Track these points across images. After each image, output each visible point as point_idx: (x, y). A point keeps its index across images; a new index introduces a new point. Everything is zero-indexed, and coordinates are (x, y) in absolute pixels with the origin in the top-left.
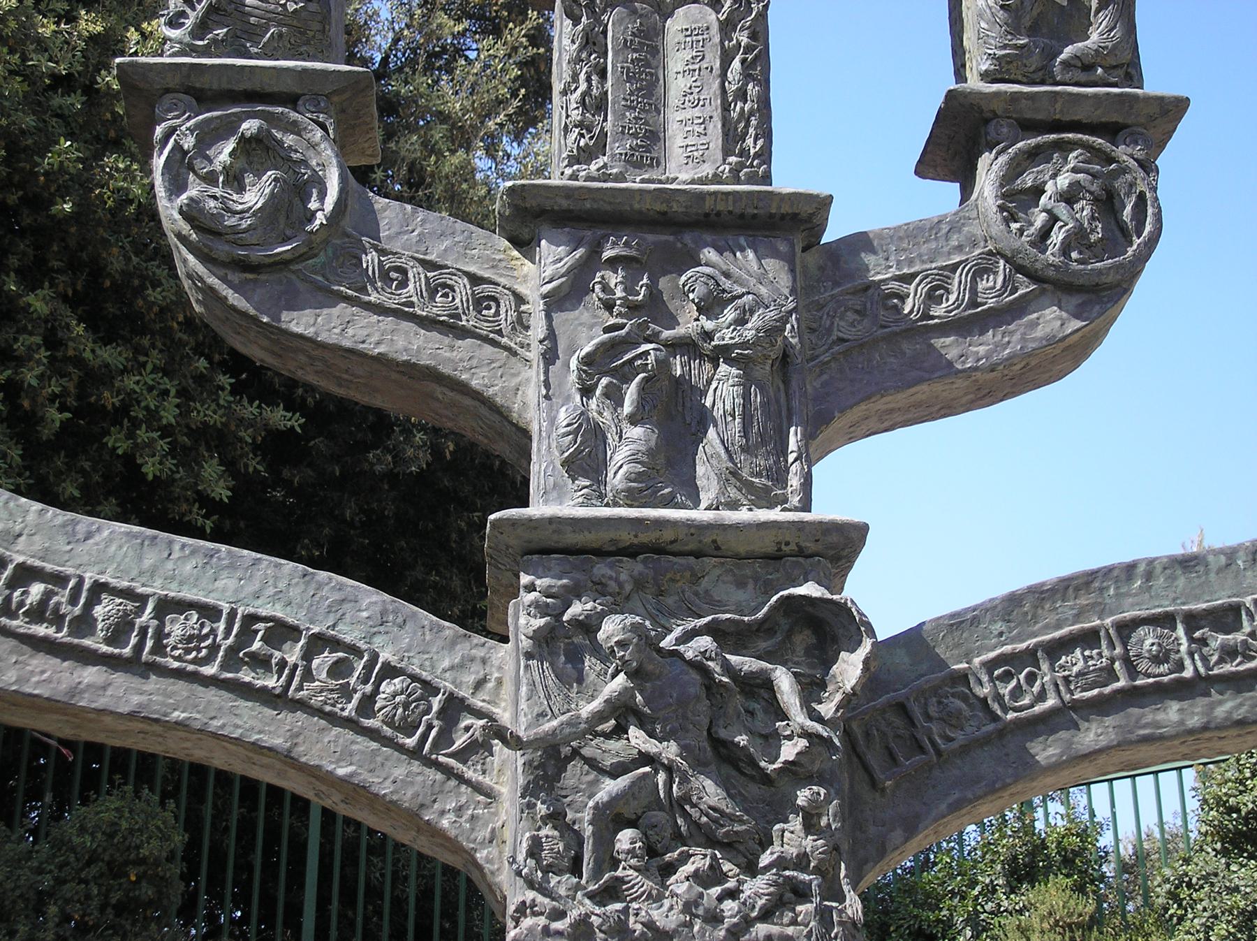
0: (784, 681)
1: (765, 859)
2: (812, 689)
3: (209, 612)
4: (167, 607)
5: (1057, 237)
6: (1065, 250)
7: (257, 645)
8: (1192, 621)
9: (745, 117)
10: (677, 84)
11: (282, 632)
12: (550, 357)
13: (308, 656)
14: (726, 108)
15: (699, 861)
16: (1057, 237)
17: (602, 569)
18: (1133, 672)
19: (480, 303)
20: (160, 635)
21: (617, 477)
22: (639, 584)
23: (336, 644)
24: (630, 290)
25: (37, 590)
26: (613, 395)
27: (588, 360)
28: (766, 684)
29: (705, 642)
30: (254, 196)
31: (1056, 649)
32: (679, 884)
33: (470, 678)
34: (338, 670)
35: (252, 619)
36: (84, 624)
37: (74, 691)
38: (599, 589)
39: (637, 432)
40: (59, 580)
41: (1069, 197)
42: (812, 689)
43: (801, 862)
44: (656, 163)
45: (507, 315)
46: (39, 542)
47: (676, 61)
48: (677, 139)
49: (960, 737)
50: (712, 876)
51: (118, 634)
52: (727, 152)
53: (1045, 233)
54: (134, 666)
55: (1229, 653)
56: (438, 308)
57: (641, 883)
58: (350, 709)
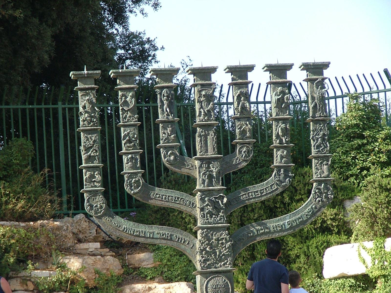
0: (220, 202)
1: (219, 216)
2: (222, 202)
3: (172, 197)
4: (169, 196)
5: (243, 156)
6: (244, 158)
7: (176, 199)
8: (254, 192)
9: (215, 147)
10: (209, 144)
11: (178, 198)
12: (199, 173)
13: (181, 200)
14: (213, 146)
15: (214, 216)
16: (243, 156)
17: (205, 193)
18: (249, 197)
19: (192, 166)
20: (169, 199)
21: (206, 185)
22: (208, 193)
23: (183, 199)
24: (206, 166)
25: (158, 195)
26: (205, 177)
27: (203, 174)
28: (219, 201)
29: (214, 199)
30: (172, 158)
31: (243, 195)
32: (213, 219)
33: (194, 201)
34: (183, 201)
35: (176, 197)
36: (162, 198)
37: (162, 204)
38: (205, 194)
39: (207, 180)
40: (160, 194)
41: (244, 152)
42: (222, 202)
43: (222, 216)
44: (208, 152)
45: (194, 168)
46: (157, 191)
47: (209, 142)
48: (209, 150)
49: (234, 204)
50: (215, 217)
51: (165, 199)
52: (214, 151)
53: (242, 155)
54: (167, 201)
55: (257, 195)
56: (188, 167)
57: (210, 219)
58: (185, 204)
